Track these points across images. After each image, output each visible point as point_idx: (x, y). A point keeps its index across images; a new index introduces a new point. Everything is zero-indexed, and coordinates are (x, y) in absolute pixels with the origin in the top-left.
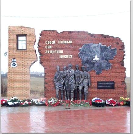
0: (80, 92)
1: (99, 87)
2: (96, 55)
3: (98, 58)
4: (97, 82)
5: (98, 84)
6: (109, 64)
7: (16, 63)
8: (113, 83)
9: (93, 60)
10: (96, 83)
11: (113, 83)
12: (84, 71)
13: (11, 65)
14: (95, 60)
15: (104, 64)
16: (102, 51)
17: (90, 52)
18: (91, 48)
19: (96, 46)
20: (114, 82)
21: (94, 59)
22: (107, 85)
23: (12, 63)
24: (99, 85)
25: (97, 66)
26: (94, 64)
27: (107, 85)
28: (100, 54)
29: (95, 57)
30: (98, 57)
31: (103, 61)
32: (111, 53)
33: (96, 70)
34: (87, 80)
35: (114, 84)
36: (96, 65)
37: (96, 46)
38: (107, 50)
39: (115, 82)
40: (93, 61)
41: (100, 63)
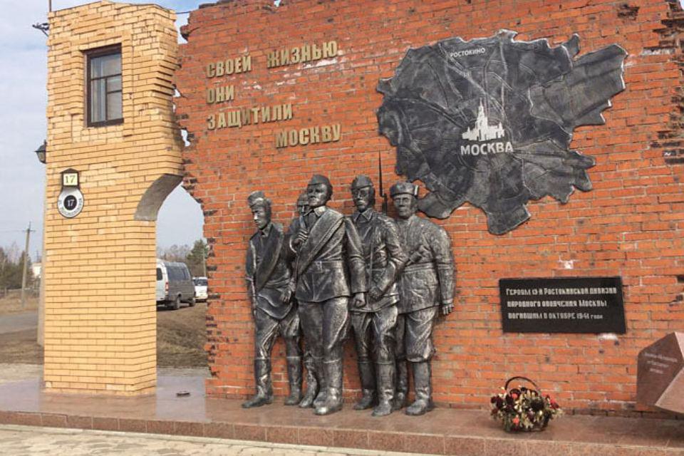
0: (384, 352)
1: (511, 316)
2: (481, 108)
3: (496, 124)
4: (496, 282)
5: (504, 298)
7: (77, 194)
8: (613, 290)
10: (496, 292)
11: (613, 290)
12: (406, 218)
13: (62, 205)
14: (478, 142)
15: (539, 160)
17: (446, 92)
18: (447, 66)
20: (615, 282)
21: (465, 136)
22: (570, 304)
23: (62, 198)
24: (511, 304)
26: (471, 160)
27: (570, 304)
29: (472, 126)
30: (491, 123)
34: (428, 269)
35: (620, 294)
37: (482, 50)
39: (625, 280)
40: (464, 150)
41: (510, 157)
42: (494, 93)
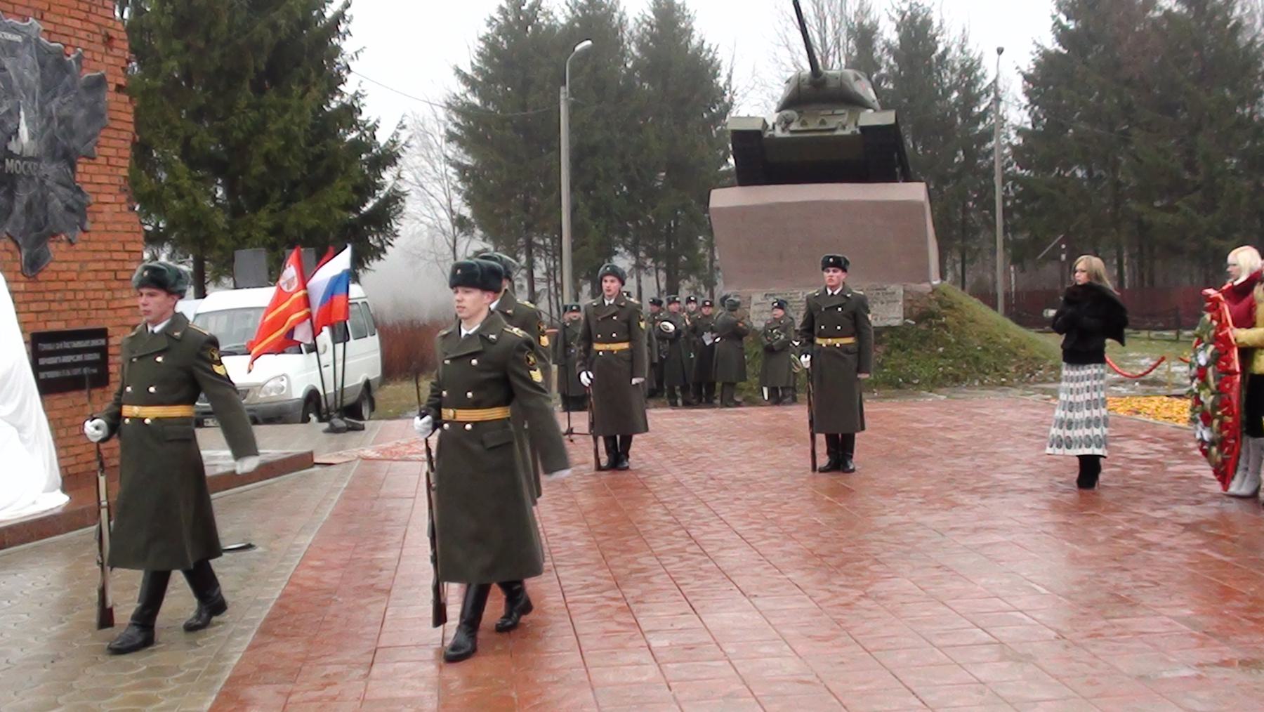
6: (79, 196)
8: (103, 342)
9: (11, 155)
11: (103, 342)
15: (60, 189)
16: (49, 88)
19: (18, 38)
20: (102, 333)
22: (79, 358)
24: (42, 361)
25: (29, 208)
27: (79, 358)
28: (42, 109)
31: (54, 166)
32: (83, 105)
33: (25, 234)
36: (23, 196)
37: (18, 38)
38: (68, 79)
42: (31, 98)
